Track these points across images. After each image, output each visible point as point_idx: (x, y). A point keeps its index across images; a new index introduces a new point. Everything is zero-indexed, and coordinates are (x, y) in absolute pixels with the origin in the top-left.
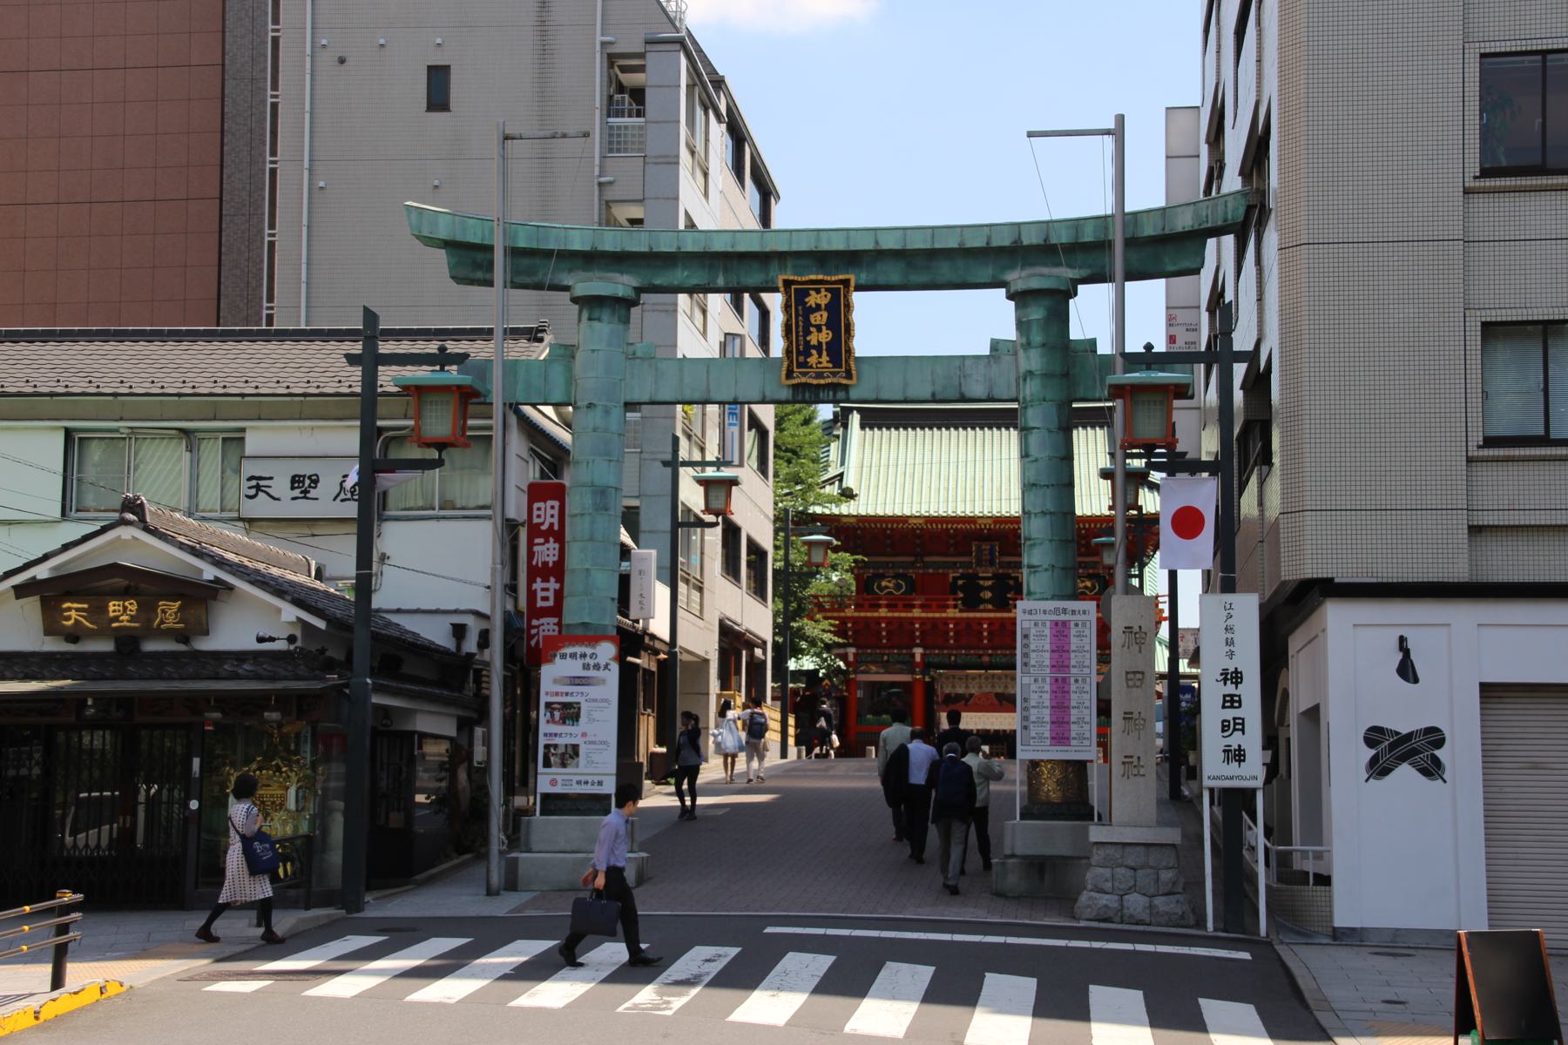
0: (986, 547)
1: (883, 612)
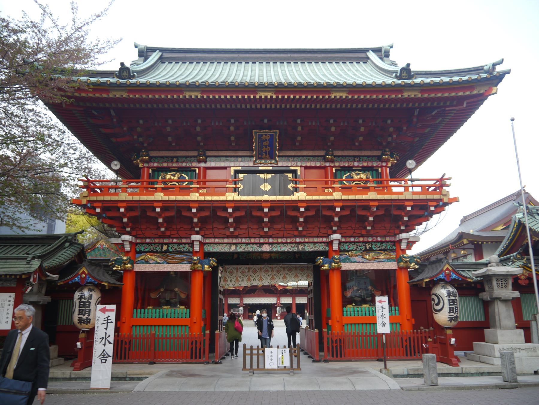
0: (266, 134)
1: (160, 196)
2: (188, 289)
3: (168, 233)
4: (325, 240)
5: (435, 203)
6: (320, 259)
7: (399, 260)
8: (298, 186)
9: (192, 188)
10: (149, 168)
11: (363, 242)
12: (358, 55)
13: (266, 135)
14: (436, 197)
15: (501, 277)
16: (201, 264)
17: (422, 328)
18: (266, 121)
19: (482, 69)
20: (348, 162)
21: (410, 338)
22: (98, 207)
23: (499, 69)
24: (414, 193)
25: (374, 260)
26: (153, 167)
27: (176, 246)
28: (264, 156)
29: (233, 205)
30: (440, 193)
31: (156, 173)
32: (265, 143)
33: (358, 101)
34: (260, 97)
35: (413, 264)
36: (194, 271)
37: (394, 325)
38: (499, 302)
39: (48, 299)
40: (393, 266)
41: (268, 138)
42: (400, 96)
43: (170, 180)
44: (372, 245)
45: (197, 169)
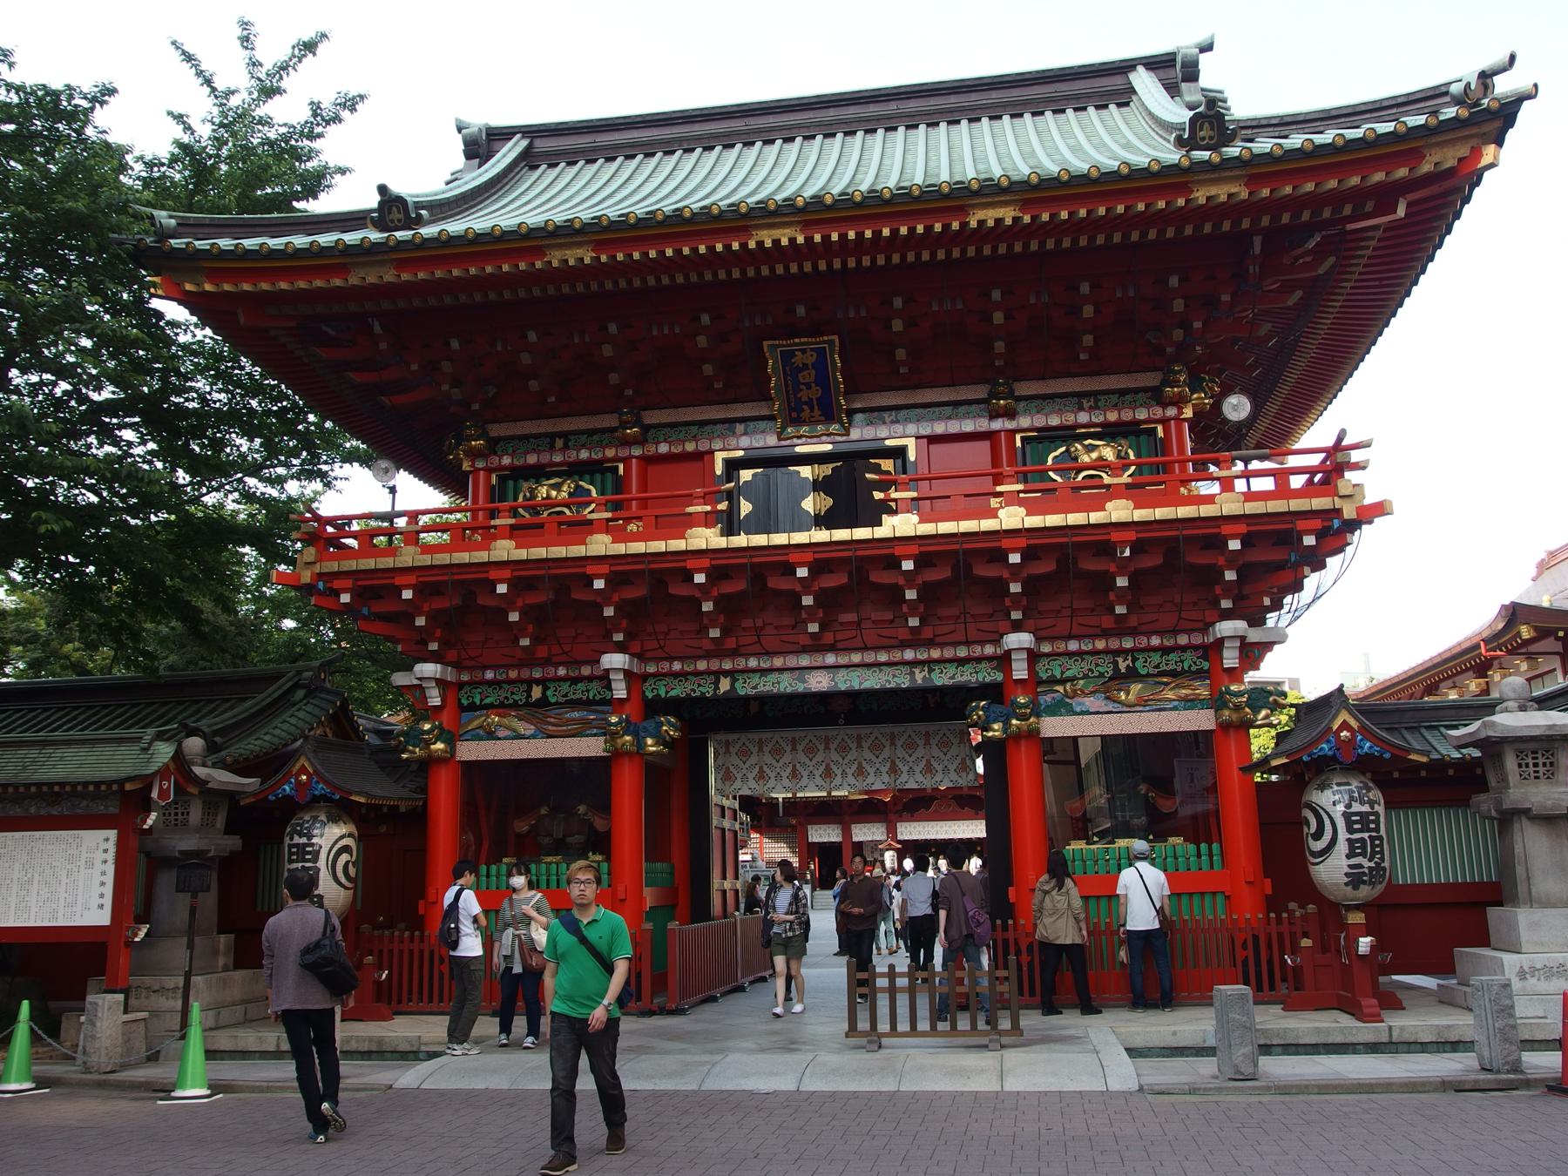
0: (804, 349)
2: (605, 806)
3: (542, 652)
4: (989, 650)
5: (1317, 524)
6: (977, 707)
7: (1218, 701)
8: (894, 495)
9: (495, 527)
10: (489, 471)
11: (1107, 652)
12: (1100, 85)
13: (804, 351)
14: (1319, 503)
15: (1533, 746)
16: (636, 734)
17: (1292, 905)
18: (801, 311)
19: (1446, 93)
20: (1060, 412)
21: (1256, 938)
22: (345, 591)
23: (1503, 86)
24: (1250, 496)
25: (1142, 703)
26: (500, 468)
27: (565, 687)
28: (806, 414)
29: (706, 563)
30: (1335, 493)
31: (511, 483)
32: (805, 377)
33: (630, 267)
34: (760, 244)
35: (1263, 713)
36: (616, 755)
37: (1092, 903)
38: (1525, 822)
39: (234, 842)
40: (1201, 720)
41: (811, 359)
42: (1181, 202)
43: (549, 503)
44: (1134, 660)
45: (621, 467)
